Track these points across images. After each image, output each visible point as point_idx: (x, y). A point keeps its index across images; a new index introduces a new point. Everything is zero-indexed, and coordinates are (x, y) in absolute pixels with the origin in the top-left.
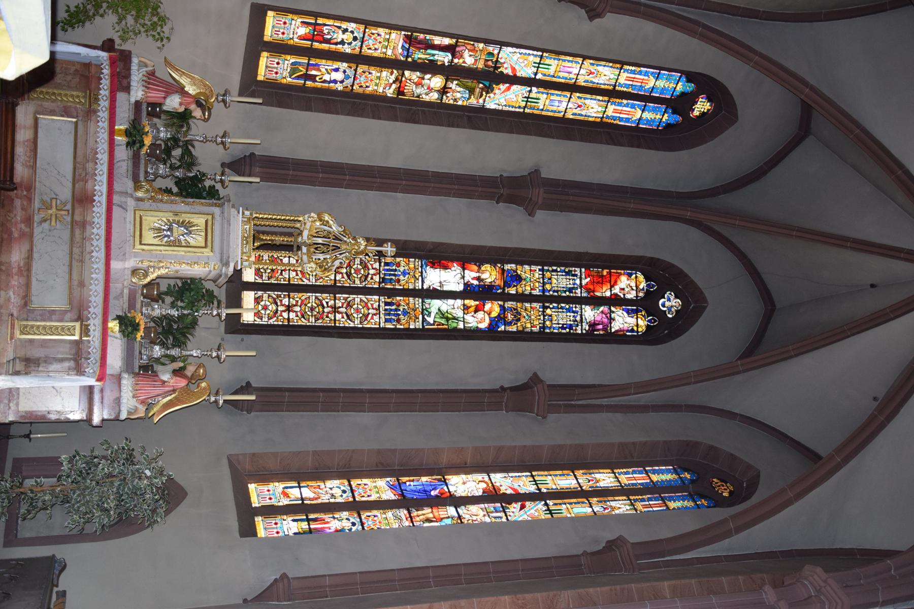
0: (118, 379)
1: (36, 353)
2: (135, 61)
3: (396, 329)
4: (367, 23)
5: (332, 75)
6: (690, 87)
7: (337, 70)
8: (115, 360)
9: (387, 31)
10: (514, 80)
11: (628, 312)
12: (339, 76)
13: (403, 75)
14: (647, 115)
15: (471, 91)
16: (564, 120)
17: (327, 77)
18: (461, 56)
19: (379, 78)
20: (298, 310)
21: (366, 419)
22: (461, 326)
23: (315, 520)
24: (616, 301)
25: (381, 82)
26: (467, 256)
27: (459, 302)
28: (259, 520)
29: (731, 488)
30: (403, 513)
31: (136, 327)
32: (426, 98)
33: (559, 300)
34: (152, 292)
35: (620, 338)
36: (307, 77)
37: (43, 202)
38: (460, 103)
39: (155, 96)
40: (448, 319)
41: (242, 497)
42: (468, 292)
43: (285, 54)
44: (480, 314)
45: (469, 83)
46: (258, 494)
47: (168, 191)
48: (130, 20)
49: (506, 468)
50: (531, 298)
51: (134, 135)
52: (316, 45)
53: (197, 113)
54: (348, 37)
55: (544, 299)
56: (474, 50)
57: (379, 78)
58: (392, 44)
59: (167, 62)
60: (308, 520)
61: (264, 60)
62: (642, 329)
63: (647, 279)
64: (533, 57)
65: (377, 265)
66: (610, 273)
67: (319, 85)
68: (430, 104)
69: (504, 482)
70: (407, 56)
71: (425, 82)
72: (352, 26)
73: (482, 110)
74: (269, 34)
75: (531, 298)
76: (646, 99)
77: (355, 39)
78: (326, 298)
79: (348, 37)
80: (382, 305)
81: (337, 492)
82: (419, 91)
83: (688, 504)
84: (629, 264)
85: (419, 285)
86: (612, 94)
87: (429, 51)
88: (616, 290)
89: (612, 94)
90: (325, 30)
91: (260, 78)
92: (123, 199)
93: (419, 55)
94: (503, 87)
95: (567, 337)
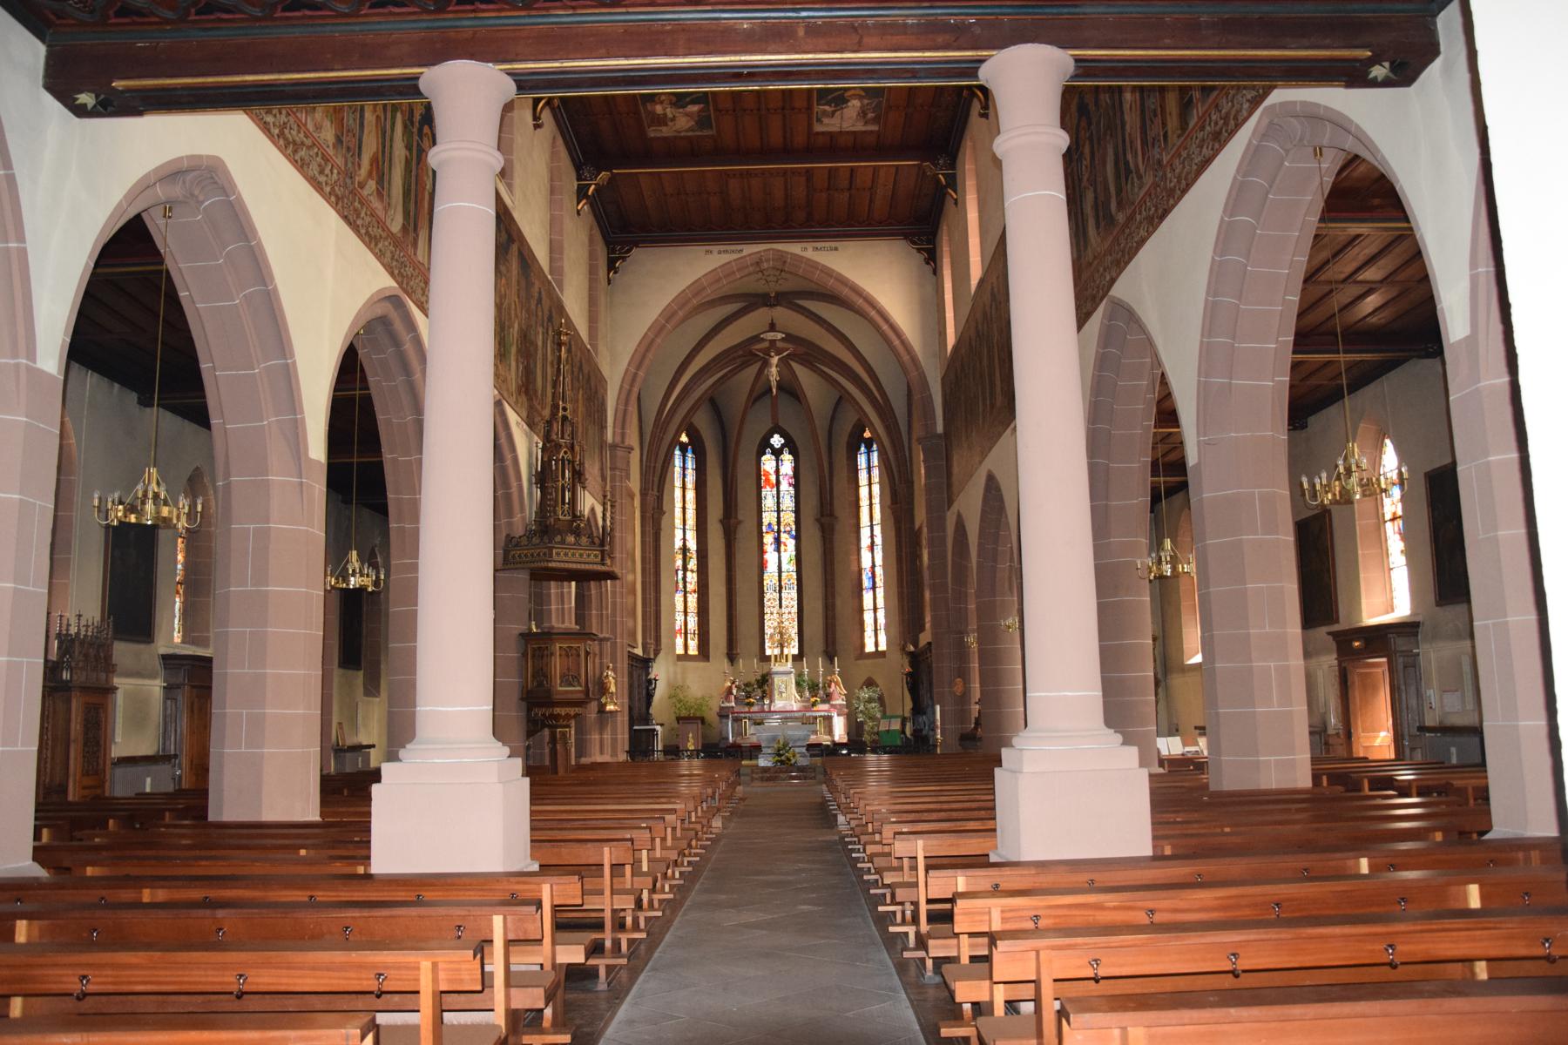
8: (825, 707)
10: (684, 539)
21: (838, 602)
24: (777, 472)
25: (693, 600)
35: (796, 470)
42: (778, 550)
55: (778, 511)
76: (684, 469)
86: (684, 488)
88: (772, 471)
89: (684, 488)
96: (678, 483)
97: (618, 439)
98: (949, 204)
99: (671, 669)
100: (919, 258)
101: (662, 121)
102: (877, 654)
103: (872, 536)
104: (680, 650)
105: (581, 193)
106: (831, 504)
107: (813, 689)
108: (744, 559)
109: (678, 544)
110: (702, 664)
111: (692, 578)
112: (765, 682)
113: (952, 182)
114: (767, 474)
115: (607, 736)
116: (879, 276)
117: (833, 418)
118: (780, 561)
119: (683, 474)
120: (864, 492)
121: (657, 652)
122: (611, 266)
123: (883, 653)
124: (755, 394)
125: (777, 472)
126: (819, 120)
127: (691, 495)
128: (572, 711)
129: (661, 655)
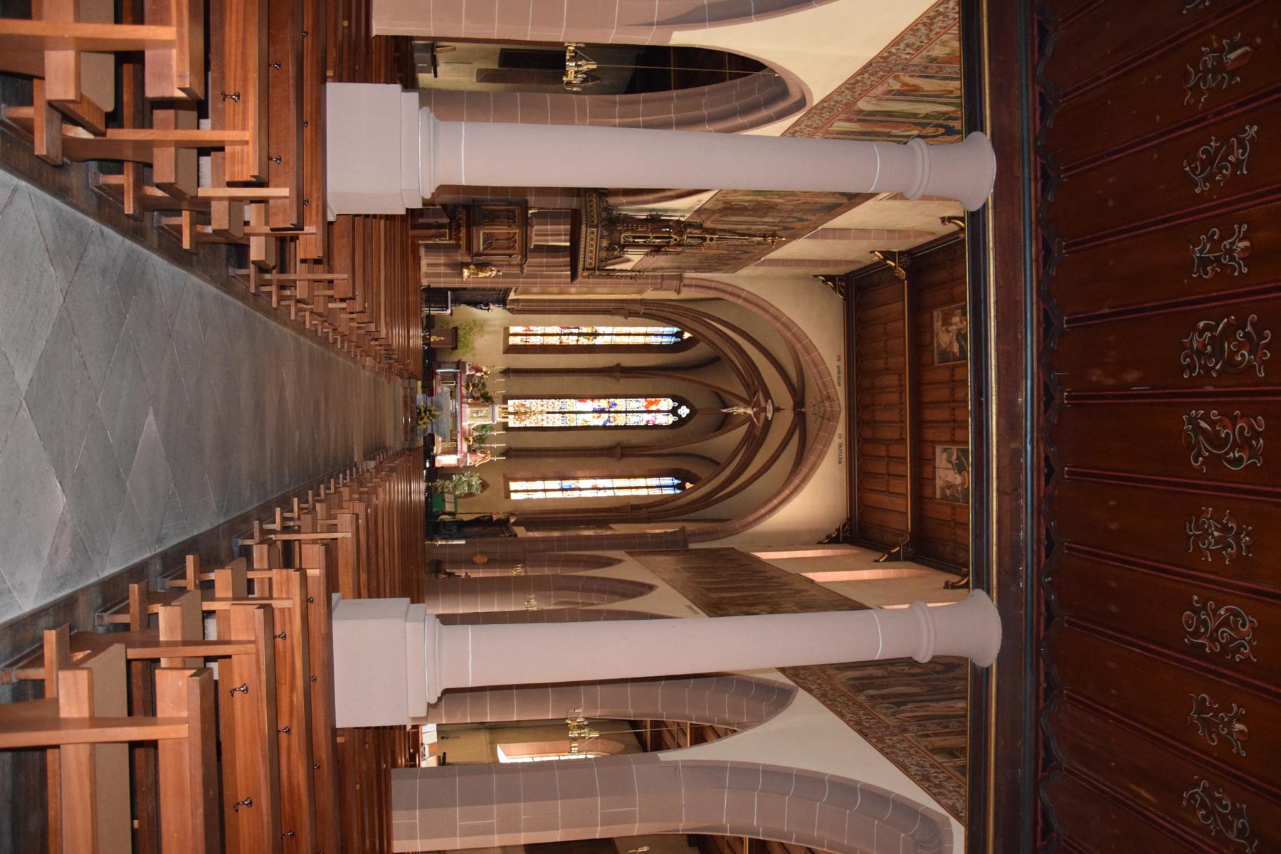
8: (465, 449)
10: (604, 335)
24: (658, 411)
25: (554, 341)
41: (507, 487)
42: (594, 411)
46: (513, 486)
55: (626, 412)
76: (662, 335)
93: (566, 331)
96: (650, 330)
97: (686, 282)
98: (876, 555)
99: (497, 322)
100: (831, 527)
101: (946, 322)
102: (508, 492)
103: (605, 489)
104: (513, 330)
105: (888, 255)
106: (632, 456)
107: (479, 440)
108: (588, 383)
109: (600, 330)
110: (501, 347)
111: (572, 341)
112: (487, 399)
113: (893, 558)
114: (657, 403)
115: (442, 270)
116: (816, 497)
117: (702, 457)
118: (584, 413)
119: (659, 334)
120: (641, 482)
121: (511, 311)
122: (828, 278)
123: (508, 497)
124: (722, 394)
125: (658, 411)
126: (945, 450)
127: (640, 340)
128: (463, 243)
129: (509, 315)
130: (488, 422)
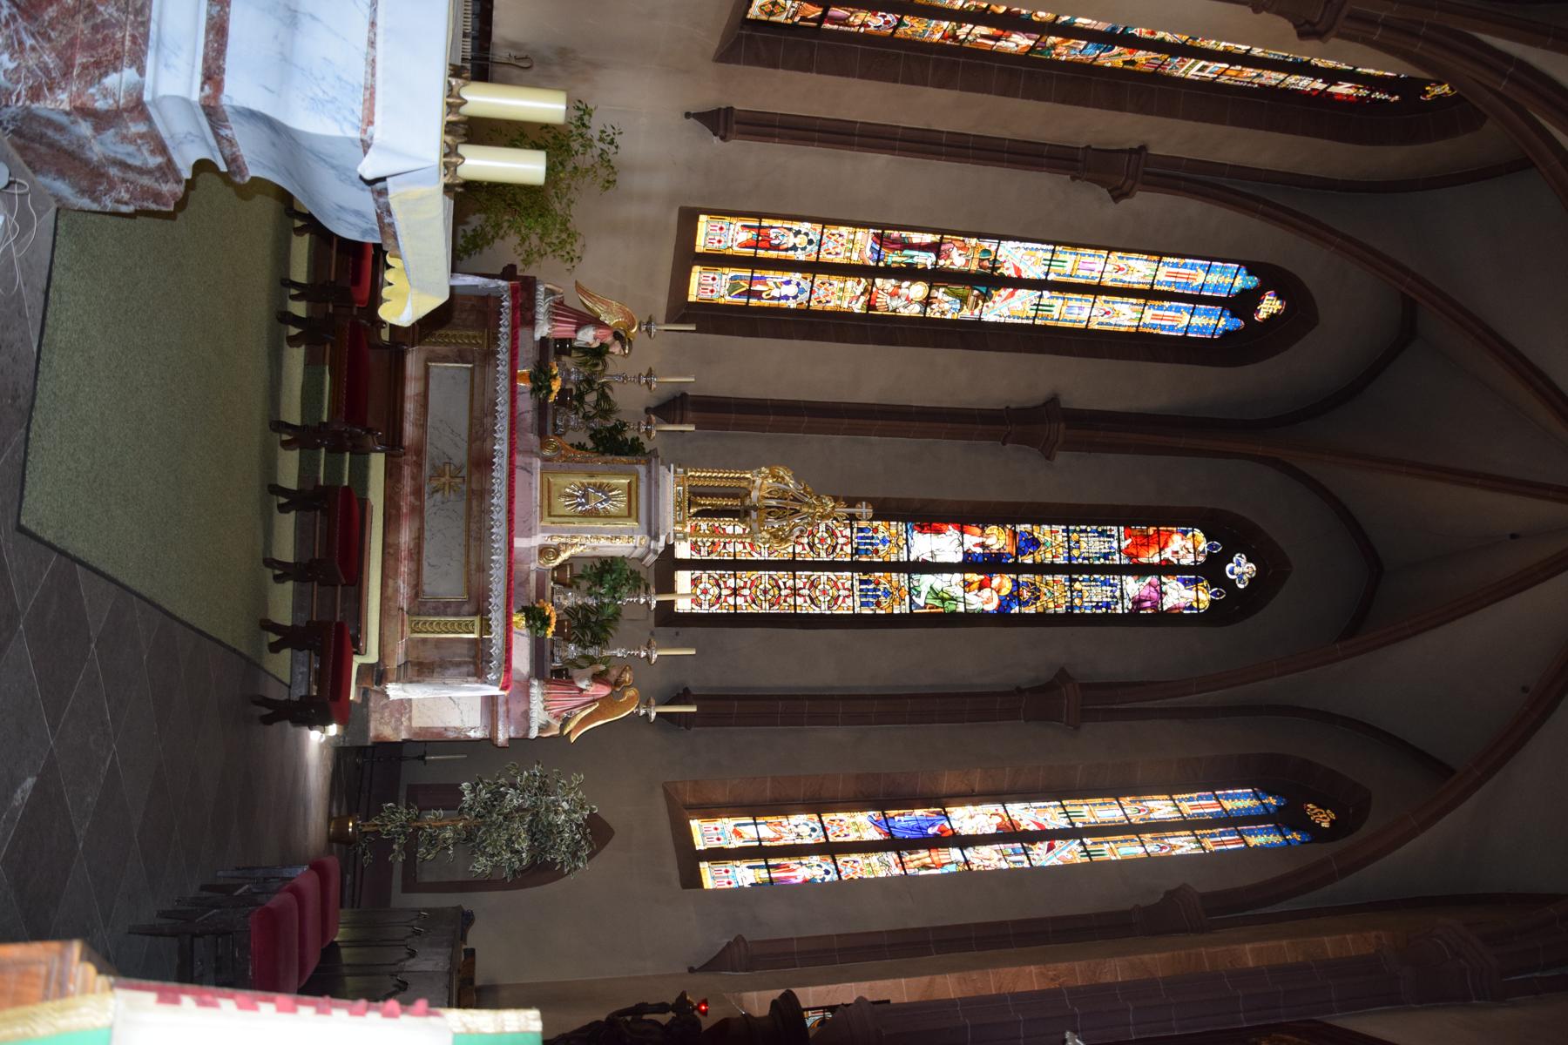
0: (526, 687)
1: (430, 655)
2: (541, 288)
3: (875, 615)
4: (825, 222)
5: (783, 290)
6: (1252, 282)
7: (788, 283)
8: (522, 661)
9: (851, 229)
10: (1019, 283)
11: (1184, 582)
12: (791, 290)
13: (873, 284)
14: (1198, 321)
15: (963, 300)
16: (1086, 332)
17: (776, 293)
18: (948, 257)
19: (843, 290)
20: (750, 595)
21: (839, 734)
22: (961, 608)
23: (777, 867)
24: (1168, 569)
25: (844, 295)
26: (966, 517)
27: (957, 577)
28: (704, 866)
29: (1333, 816)
30: (891, 857)
31: (546, 621)
32: (904, 312)
33: (1090, 569)
34: (568, 576)
35: (1175, 618)
36: (750, 294)
37: (434, 467)
38: (949, 316)
39: (565, 330)
40: (943, 600)
41: (684, 837)
42: (969, 564)
43: (722, 266)
44: (986, 592)
45: (960, 289)
46: (703, 833)
47: (581, 447)
48: (535, 240)
49: (1027, 795)
50: (1053, 569)
51: (540, 378)
52: (761, 253)
53: (616, 349)
54: (801, 241)
55: (1071, 569)
56: (965, 248)
57: (843, 290)
58: (858, 246)
59: (579, 288)
60: (768, 867)
61: (697, 274)
62: (1204, 604)
63: (1208, 538)
64: (1042, 252)
65: (847, 532)
66: (1158, 532)
67: (765, 303)
68: (910, 319)
69: (1026, 815)
70: (878, 260)
71: (903, 291)
72: (805, 227)
73: (979, 323)
74: (701, 245)
75: (1053, 569)
76: (1196, 299)
77: (810, 242)
78: (783, 577)
79: (801, 241)
80: (856, 583)
81: (805, 831)
82: (894, 303)
83: (1275, 839)
84: (1184, 519)
85: (903, 557)
86: (1150, 294)
87: (906, 252)
88: (1167, 554)
89: (1150, 294)
90: (772, 233)
91: (692, 298)
92: (528, 460)
93: (894, 258)
94: (1004, 292)
95: (1103, 620)
99: (660, 183)
102: (690, 859)
103: (1048, 836)
107: (589, 615)
111: (906, 299)
112: (613, 444)
118: (940, 566)
123: (696, 881)
125: (1168, 569)
127: (1125, 316)
130: (621, 547)
